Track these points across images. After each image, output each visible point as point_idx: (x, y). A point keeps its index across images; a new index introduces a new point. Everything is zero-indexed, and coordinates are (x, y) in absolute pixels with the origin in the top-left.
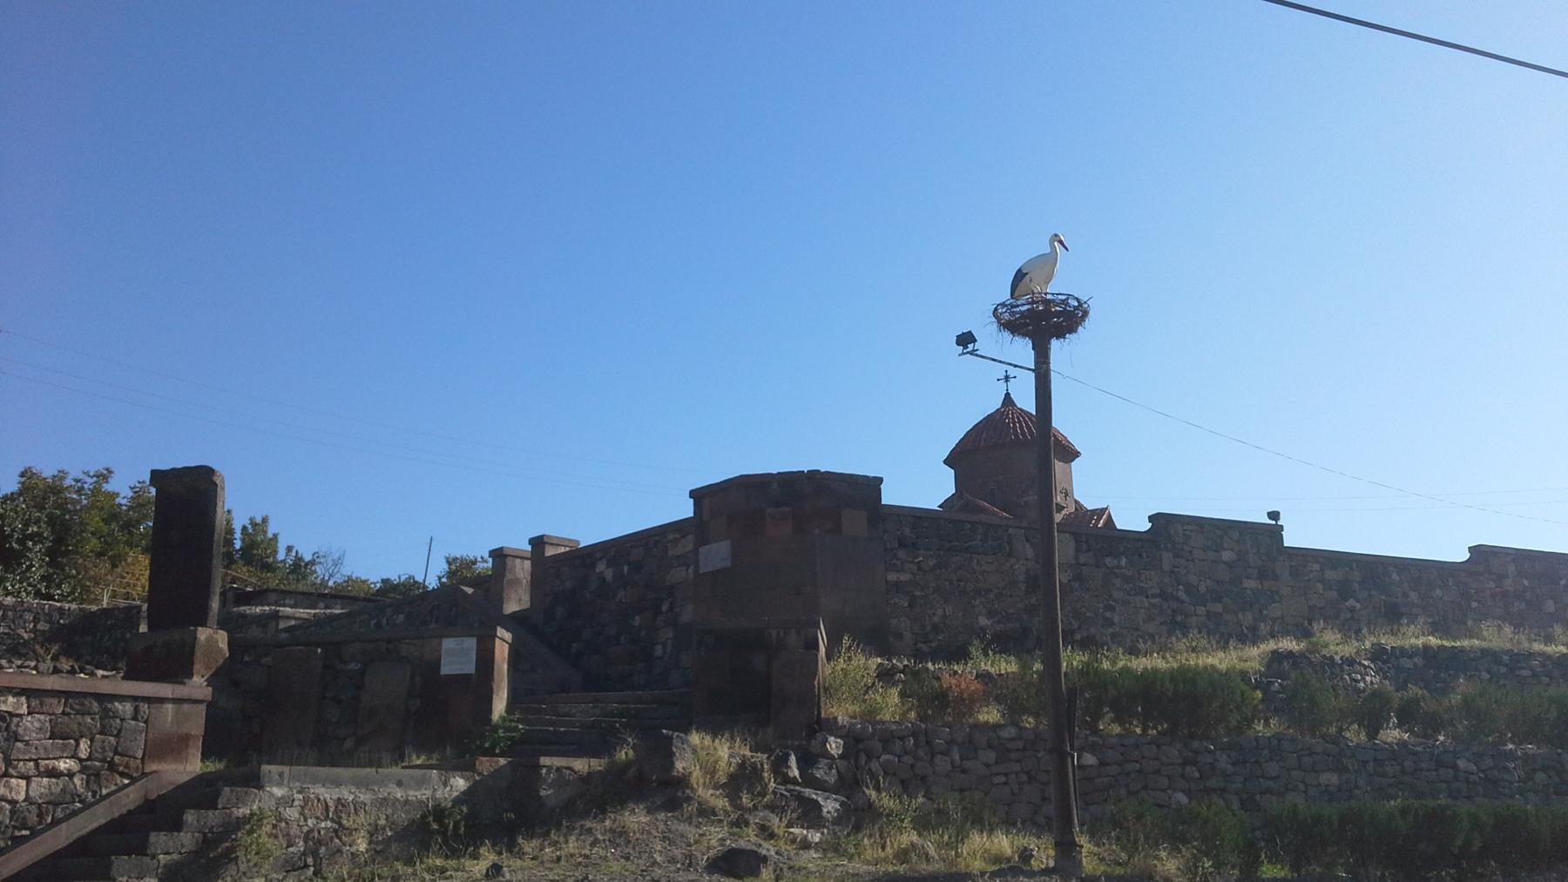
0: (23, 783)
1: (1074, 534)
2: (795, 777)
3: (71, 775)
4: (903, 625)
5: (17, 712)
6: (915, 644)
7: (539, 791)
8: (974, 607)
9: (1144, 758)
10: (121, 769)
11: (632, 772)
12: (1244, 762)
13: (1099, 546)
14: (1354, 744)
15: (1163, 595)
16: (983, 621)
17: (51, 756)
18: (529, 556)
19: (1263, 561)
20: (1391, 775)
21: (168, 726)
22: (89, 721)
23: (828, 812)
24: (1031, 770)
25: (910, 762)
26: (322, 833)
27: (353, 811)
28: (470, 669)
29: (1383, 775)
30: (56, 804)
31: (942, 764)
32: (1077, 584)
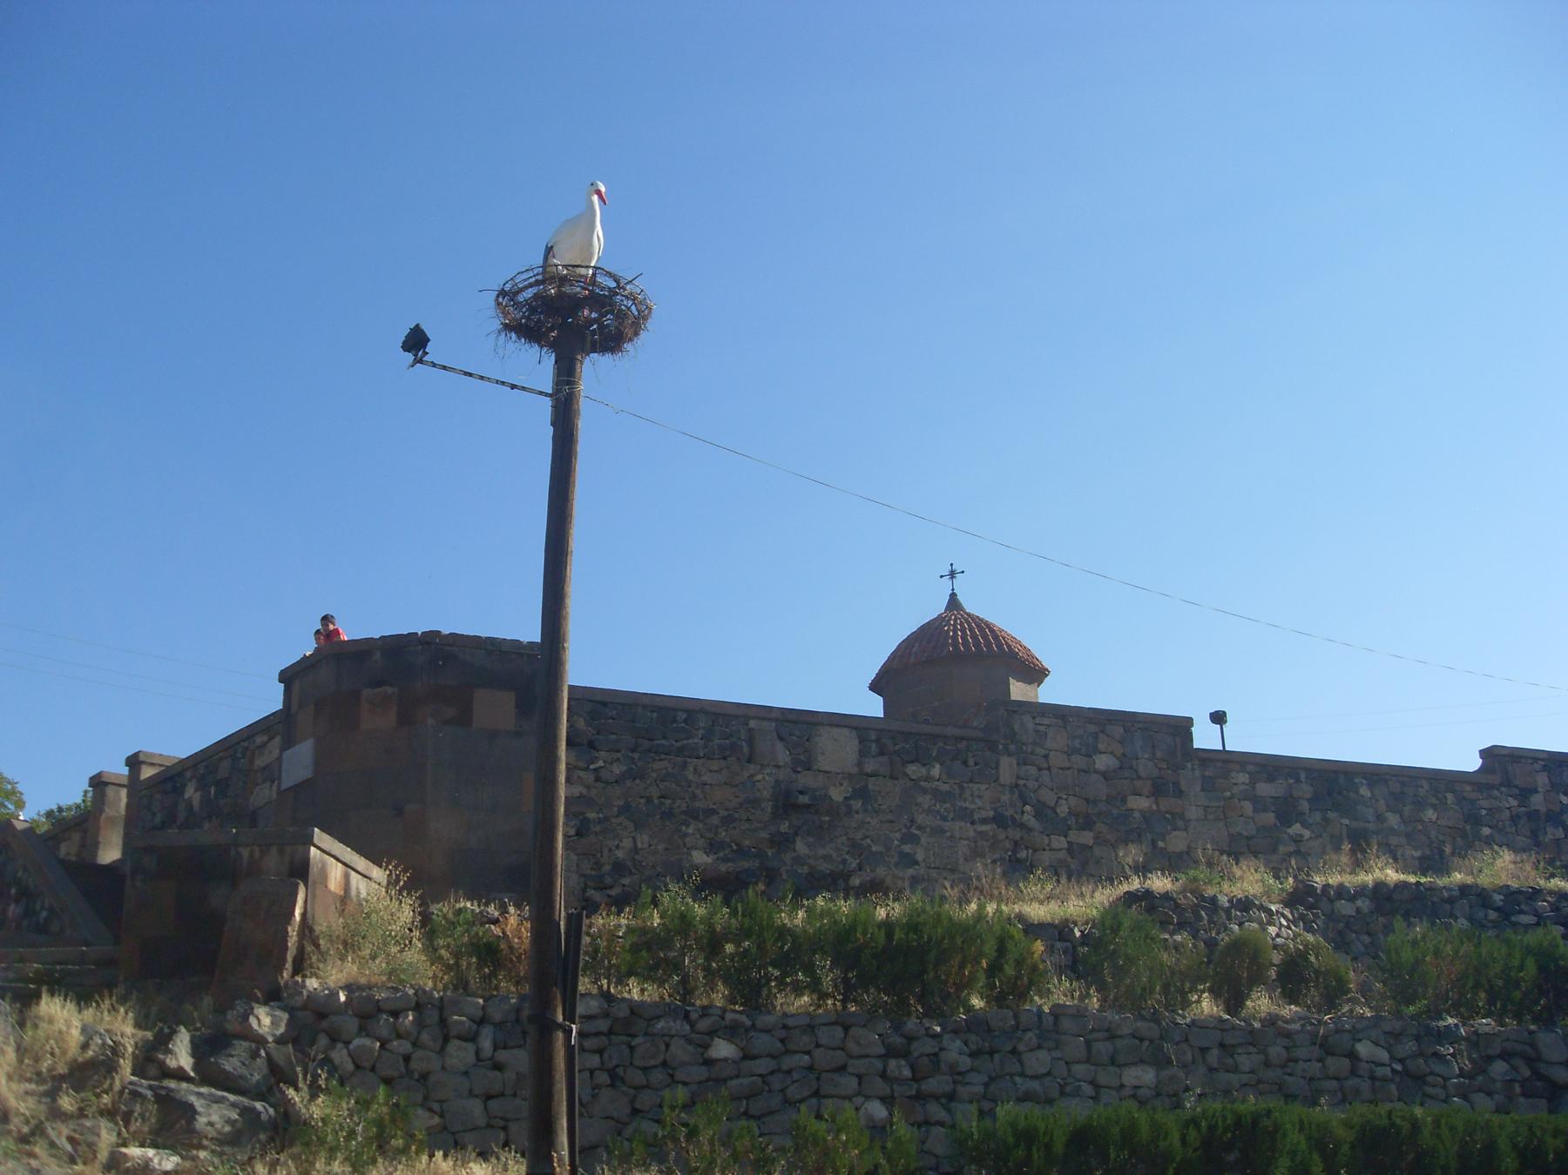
1: (856, 728)
2: (181, 1069)
6: (584, 891)
8: (686, 835)
9: (818, 1046)
12: (991, 1053)
13: (897, 747)
14: (1188, 1020)
15: (999, 820)
16: (699, 857)
19: (1160, 769)
20: (1247, 1069)
23: (211, 1124)
24: (617, 1066)
25: (401, 1050)
29: (1235, 1069)
31: (459, 1054)
32: (860, 804)
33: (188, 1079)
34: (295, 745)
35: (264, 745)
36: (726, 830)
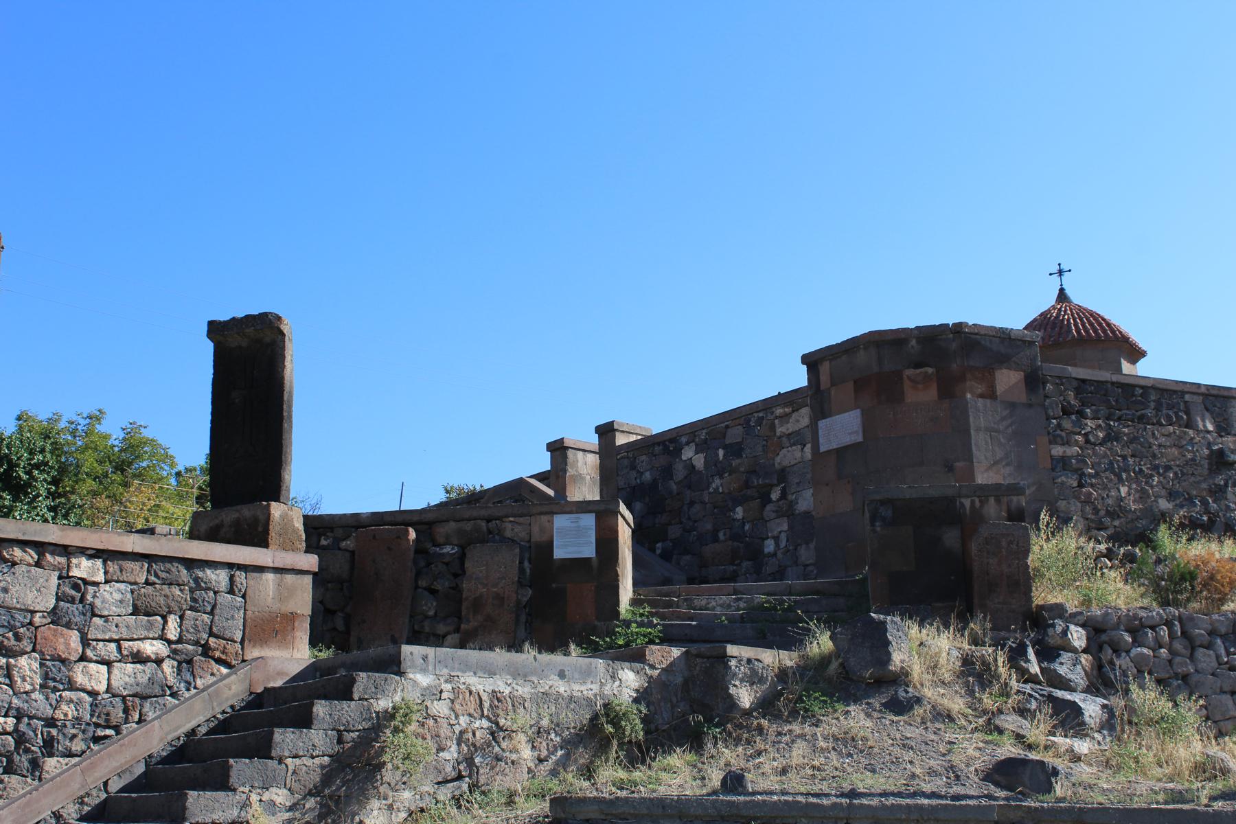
0: (104, 668)
2: (1037, 674)
3: (159, 662)
4: (1073, 508)
5: (93, 579)
7: (729, 689)
10: (217, 654)
11: (834, 665)
17: (135, 637)
18: (596, 448)
21: (269, 600)
22: (178, 592)
26: (478, 734)
27: (510, 707)
28: (588, 550)
30: (144, 698)
31: (1205, 659)
33: (1039, 683)
34: (830, 416)
35: (788, 415)
36: (1179, 483)
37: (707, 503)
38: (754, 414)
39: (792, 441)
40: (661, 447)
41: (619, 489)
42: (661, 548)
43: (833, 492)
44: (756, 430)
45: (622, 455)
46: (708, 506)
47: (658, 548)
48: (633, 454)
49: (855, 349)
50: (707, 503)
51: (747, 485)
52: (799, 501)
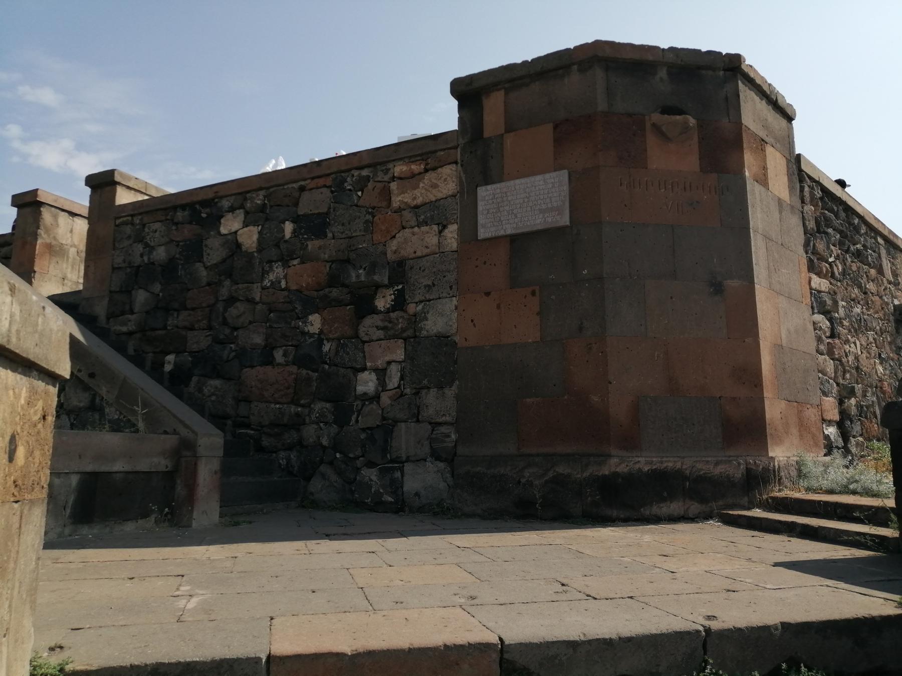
18: (85, 212)
34: (501, 180)
37: (257, 303)
38: (353, 172)
39: (423, 217)
40: (186, 213)
41: (114, 269)
42: (173, 362)
43: (498, 307)
44: (355, 197)
45: (125, 219)
46: (259, 307)
47: (169, 362)
48: (141, 220)
49: (561, 72)
50: (257, 303)
51: (334, 280)
52: (429, 316)
